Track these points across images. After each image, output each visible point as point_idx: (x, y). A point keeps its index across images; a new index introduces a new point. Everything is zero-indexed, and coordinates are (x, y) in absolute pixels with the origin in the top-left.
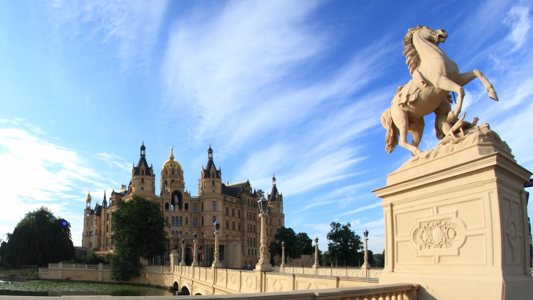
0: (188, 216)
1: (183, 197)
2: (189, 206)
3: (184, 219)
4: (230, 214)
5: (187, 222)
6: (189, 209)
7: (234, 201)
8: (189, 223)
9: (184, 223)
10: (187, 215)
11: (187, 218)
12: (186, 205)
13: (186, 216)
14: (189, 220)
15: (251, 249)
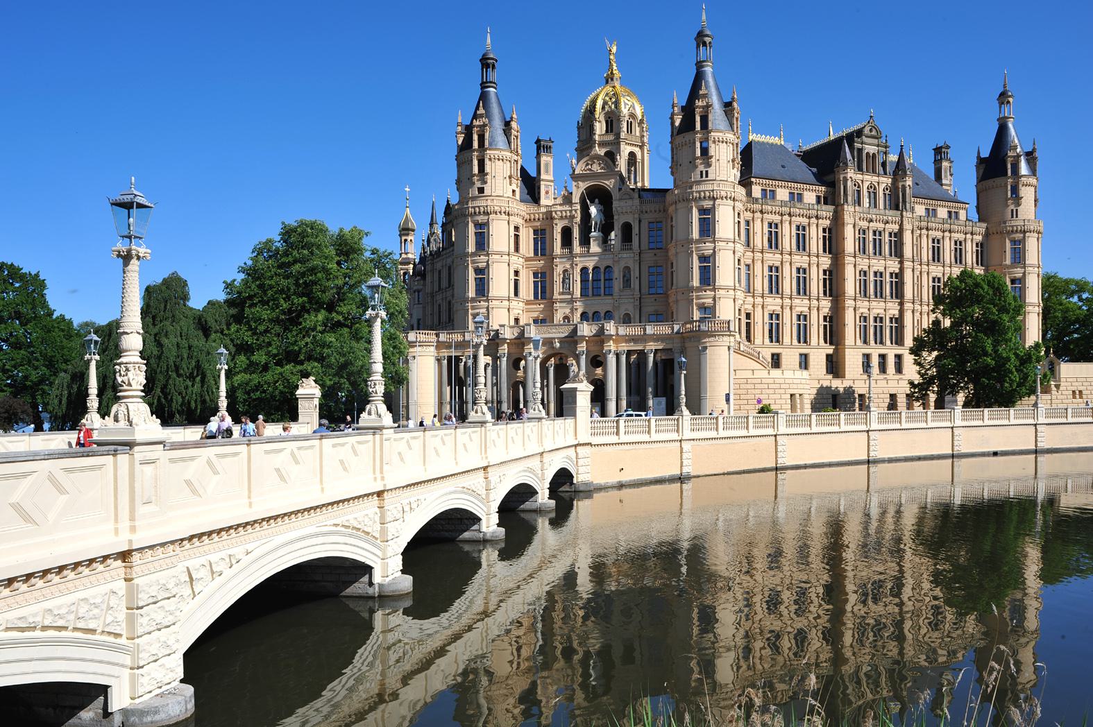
0: (631, 264)
1: (615, 204)
2: (635, 230)
3: (617, 274)
4: (788, 241)
5: (627, 282)
6: (635, 239)
7: (810, 197)
8: (635, 283)
9: (617, 284)
10: (628, 259)
11: (627, 269)
12: (627, 230)
13: (623, 264)
14: (635, 273)
15: (875, 353)
